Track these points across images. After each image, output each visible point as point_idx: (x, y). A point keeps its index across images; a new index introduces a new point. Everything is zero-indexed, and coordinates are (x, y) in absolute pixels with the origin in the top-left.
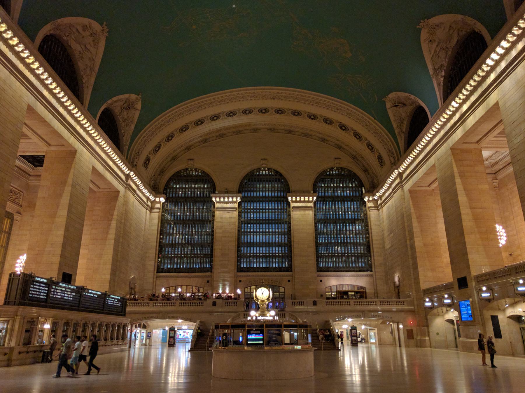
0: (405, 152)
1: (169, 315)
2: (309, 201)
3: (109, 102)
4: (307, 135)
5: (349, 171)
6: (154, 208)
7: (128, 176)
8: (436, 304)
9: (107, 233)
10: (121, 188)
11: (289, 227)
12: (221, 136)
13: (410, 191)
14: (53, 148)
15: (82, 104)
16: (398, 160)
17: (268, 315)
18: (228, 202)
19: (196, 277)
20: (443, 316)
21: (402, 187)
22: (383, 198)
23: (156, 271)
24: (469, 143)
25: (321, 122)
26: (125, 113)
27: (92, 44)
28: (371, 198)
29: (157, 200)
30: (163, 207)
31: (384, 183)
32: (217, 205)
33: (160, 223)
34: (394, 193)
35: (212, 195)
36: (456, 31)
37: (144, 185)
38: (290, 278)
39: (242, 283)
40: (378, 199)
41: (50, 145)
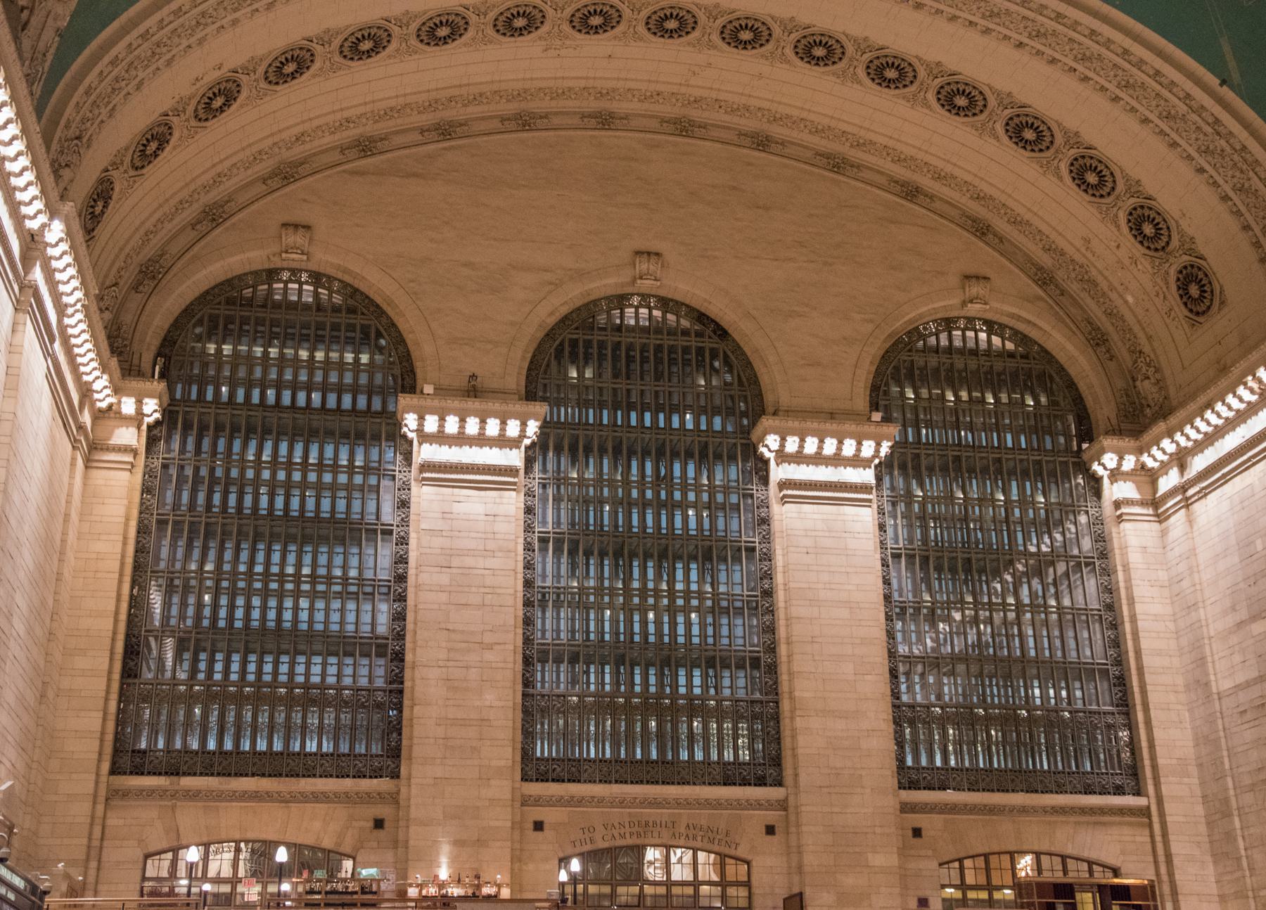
5: (1021, 338)
12: (445, 131)
18: (481, 440)
19: (317, 797)
23: (106, 766)
28: (1129, 463)
29: (128, 406)
32: (426, 453)
33: (133, 524)
38: (772, 816)
39: (548, 833)
40: (1165, 467)
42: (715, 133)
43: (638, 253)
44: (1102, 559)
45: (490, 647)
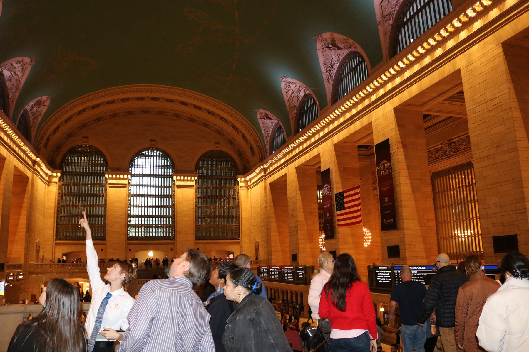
2: (191, 180)
6: (52, 182)
7: (35, 163)
11: (173, 201)
13: (271, 184)
22: (253, 181)
29: (55, 174)
31: (253, 172)
32: (110, 181)
34: (260, 182)
37: (46, 166)
43: (151, 140)
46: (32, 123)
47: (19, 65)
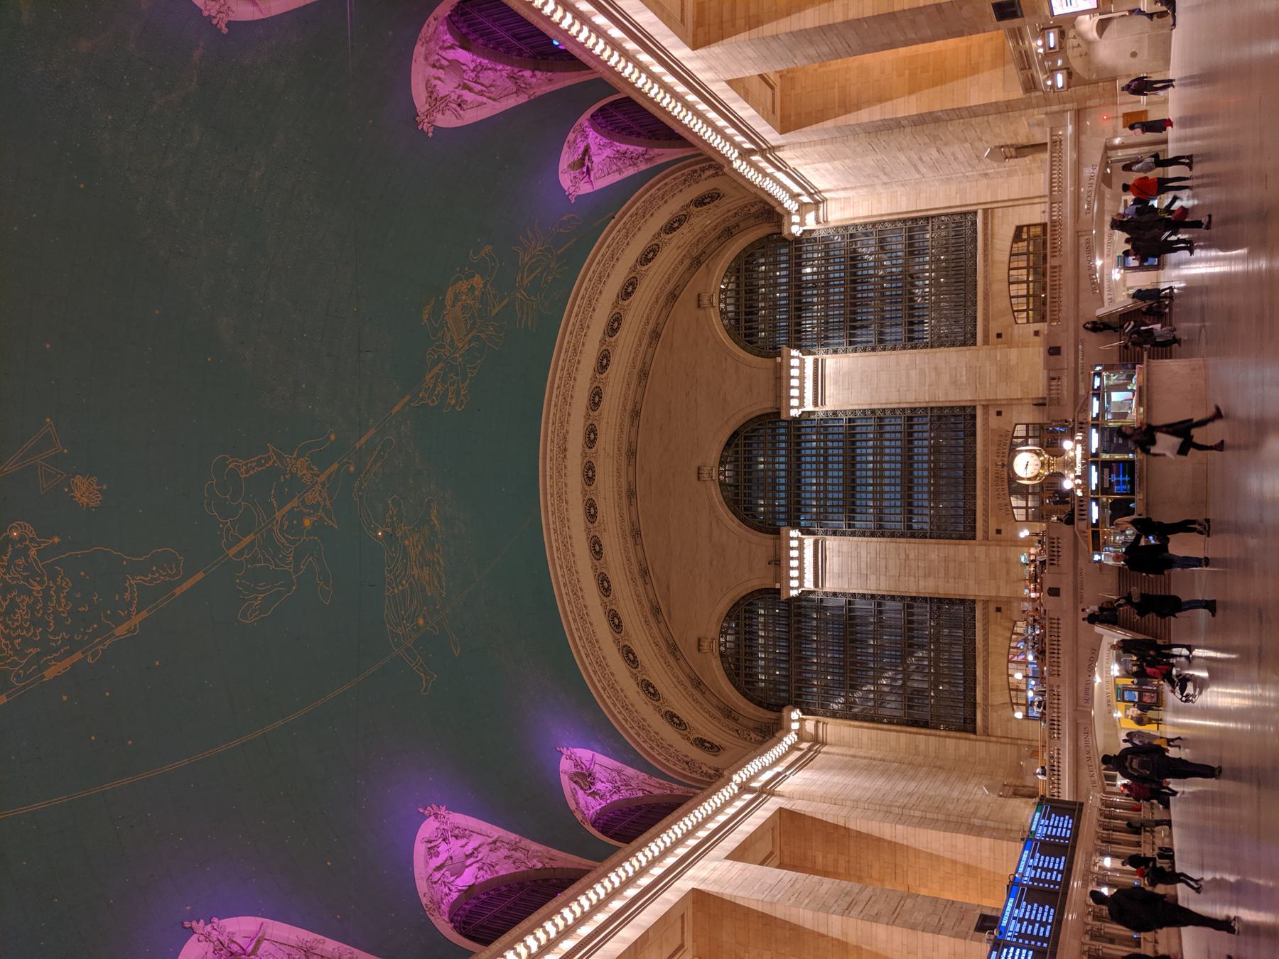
0: (692, 146)
1: (1081, 702)
2: (802, 367)
3: (579, 817)
4: (644, 374)
7: (744, 788)
8: (1060, 62)
9: (879, 839)
10: (772, 805)
12: (644, 572)
14: (689, 943)
15: (587, 872)
16: (710, 159)
17: (1072, 454)
18: (801, 559)
19: (986, 639)
20: (1089, 43)
21: (773, 149)
22: (796, 189)
23: (972, 736)
24: (682, 10)
25: (616, 341)
26: (599, 786)
27: (465, 841)
29: (795, 726)
30: (813, 714)
32: (809, 585)
33: (853, 723)
34: (786, 166)
35: (784, 597)
36: (444, 54)
37: (762, 754)
38: (993, 412)
39: (1002, 527)
41: (682, 946)
42: (633, 439)
44: (851, 233)
45: (907, 556)
46: (640, 794)
47: (443, 847)
